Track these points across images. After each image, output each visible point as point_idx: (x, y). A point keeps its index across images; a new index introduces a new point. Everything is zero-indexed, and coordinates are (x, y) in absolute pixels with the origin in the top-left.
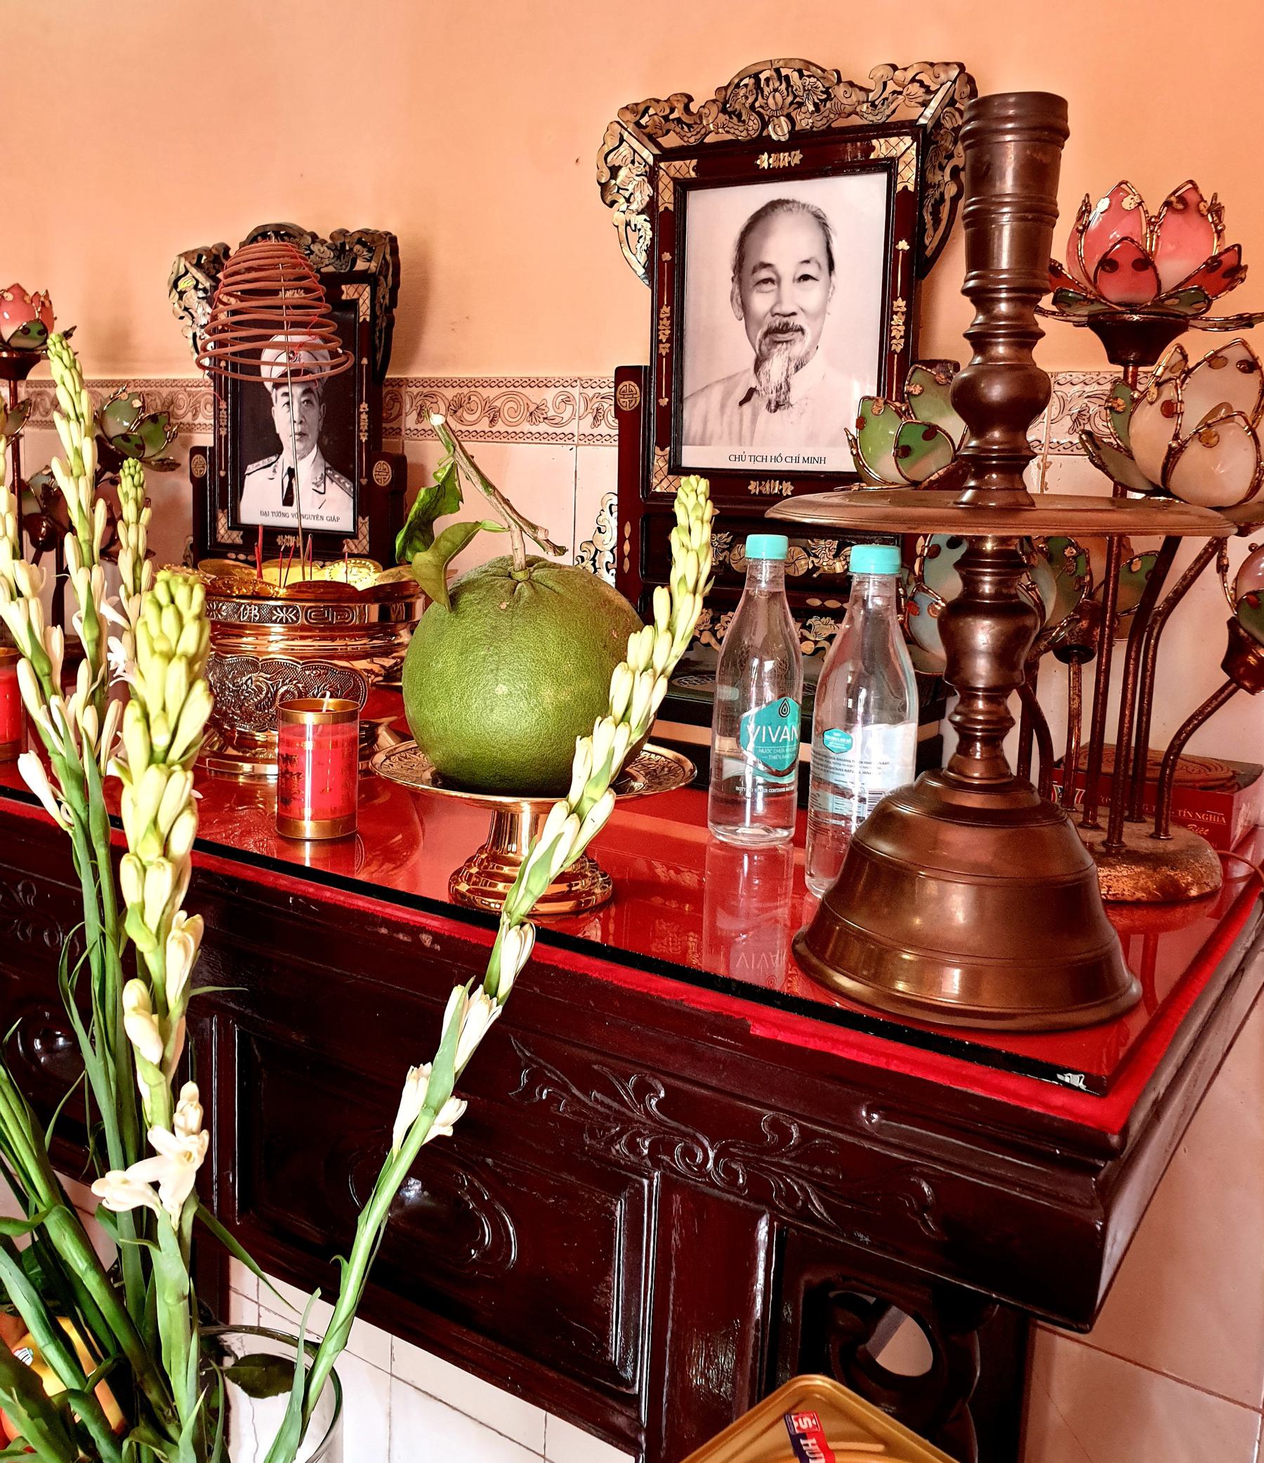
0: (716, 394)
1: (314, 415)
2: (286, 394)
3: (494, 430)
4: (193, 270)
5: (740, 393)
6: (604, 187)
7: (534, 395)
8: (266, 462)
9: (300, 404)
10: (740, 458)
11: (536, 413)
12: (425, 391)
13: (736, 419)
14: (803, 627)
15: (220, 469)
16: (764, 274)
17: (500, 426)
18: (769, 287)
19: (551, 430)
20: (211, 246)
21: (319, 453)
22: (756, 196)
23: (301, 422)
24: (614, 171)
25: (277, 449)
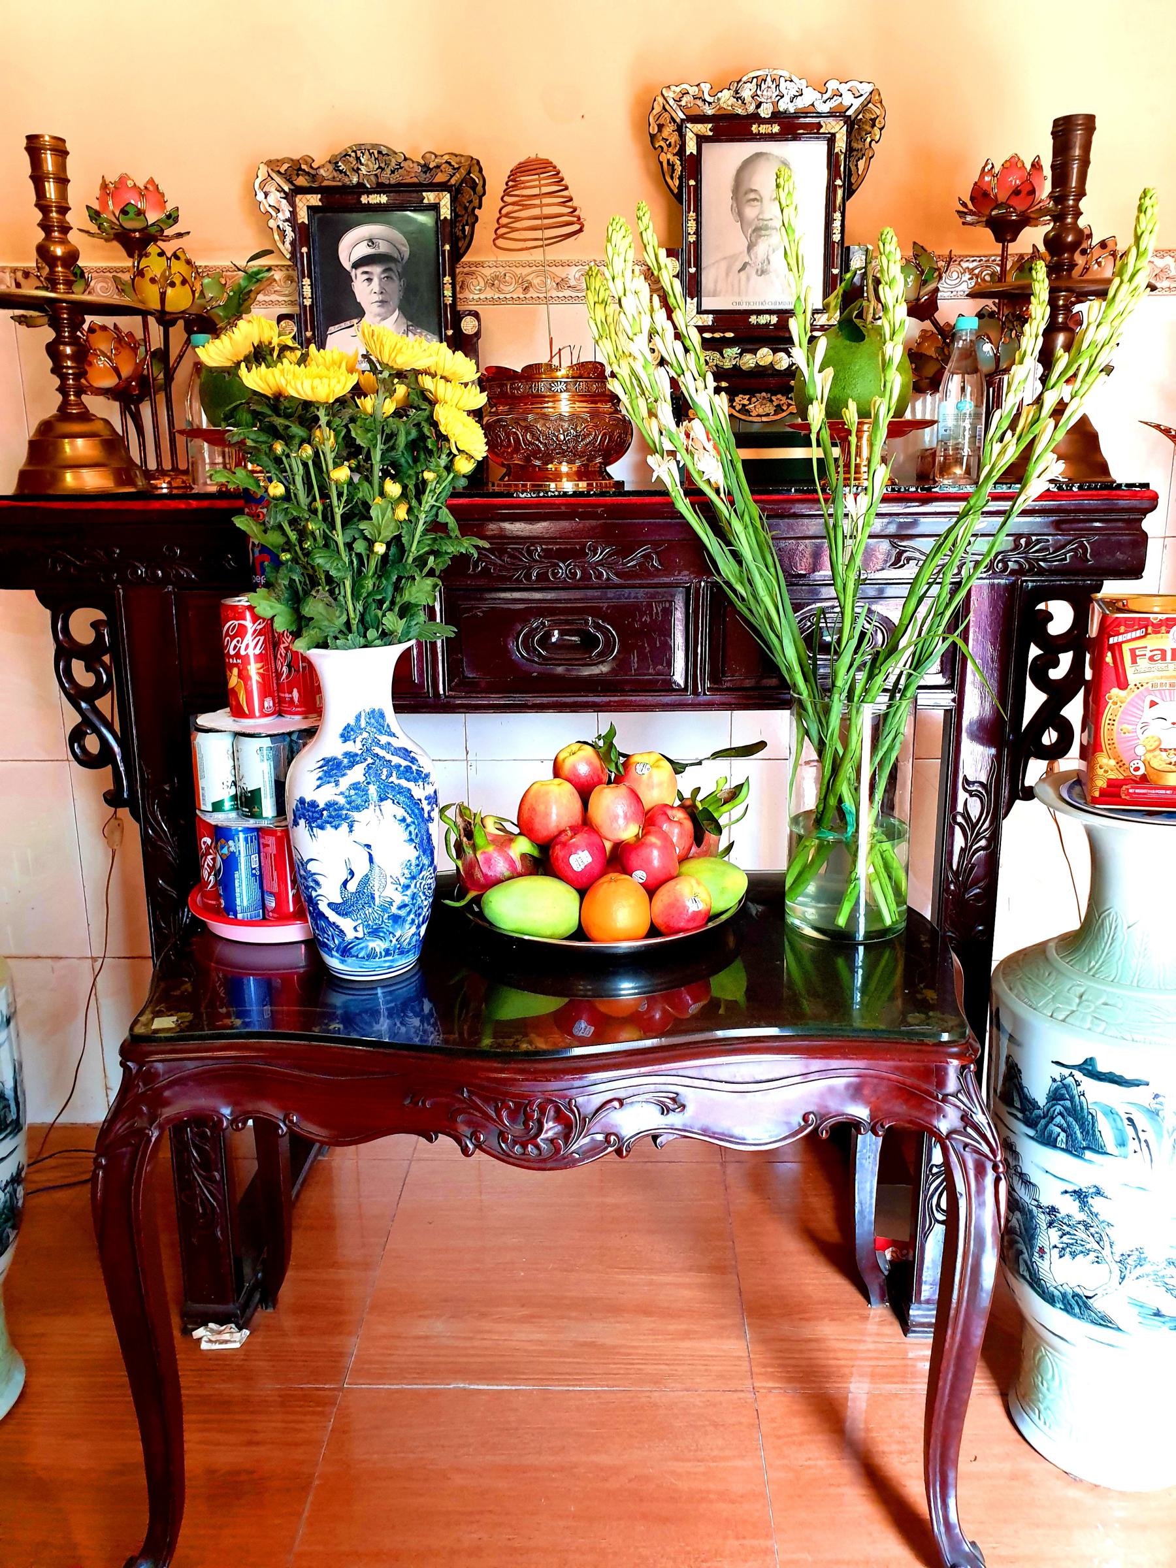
0: (723, 265)
1: (395, 287)
2: (366, 273)
3: (528, 296)
4: (274, 175)
5: (739, 265)
6: (653, 137)
7: (560, 272)
8: (348, 323)
9: (380, 280)
10: (740, 303)
11: (561, 284)
12: (466, 270)
13: (736, 283)
14: (787, 398)
15: (306, 330)
16: (752, 196)
17: (532, 293)
18: (756, 203)
19: (574, 294)
20: (298, 158)
21: (401, 315)
22: (745, 150)
23: (382, 293)
24: (661, 127)
25: (360, 313)
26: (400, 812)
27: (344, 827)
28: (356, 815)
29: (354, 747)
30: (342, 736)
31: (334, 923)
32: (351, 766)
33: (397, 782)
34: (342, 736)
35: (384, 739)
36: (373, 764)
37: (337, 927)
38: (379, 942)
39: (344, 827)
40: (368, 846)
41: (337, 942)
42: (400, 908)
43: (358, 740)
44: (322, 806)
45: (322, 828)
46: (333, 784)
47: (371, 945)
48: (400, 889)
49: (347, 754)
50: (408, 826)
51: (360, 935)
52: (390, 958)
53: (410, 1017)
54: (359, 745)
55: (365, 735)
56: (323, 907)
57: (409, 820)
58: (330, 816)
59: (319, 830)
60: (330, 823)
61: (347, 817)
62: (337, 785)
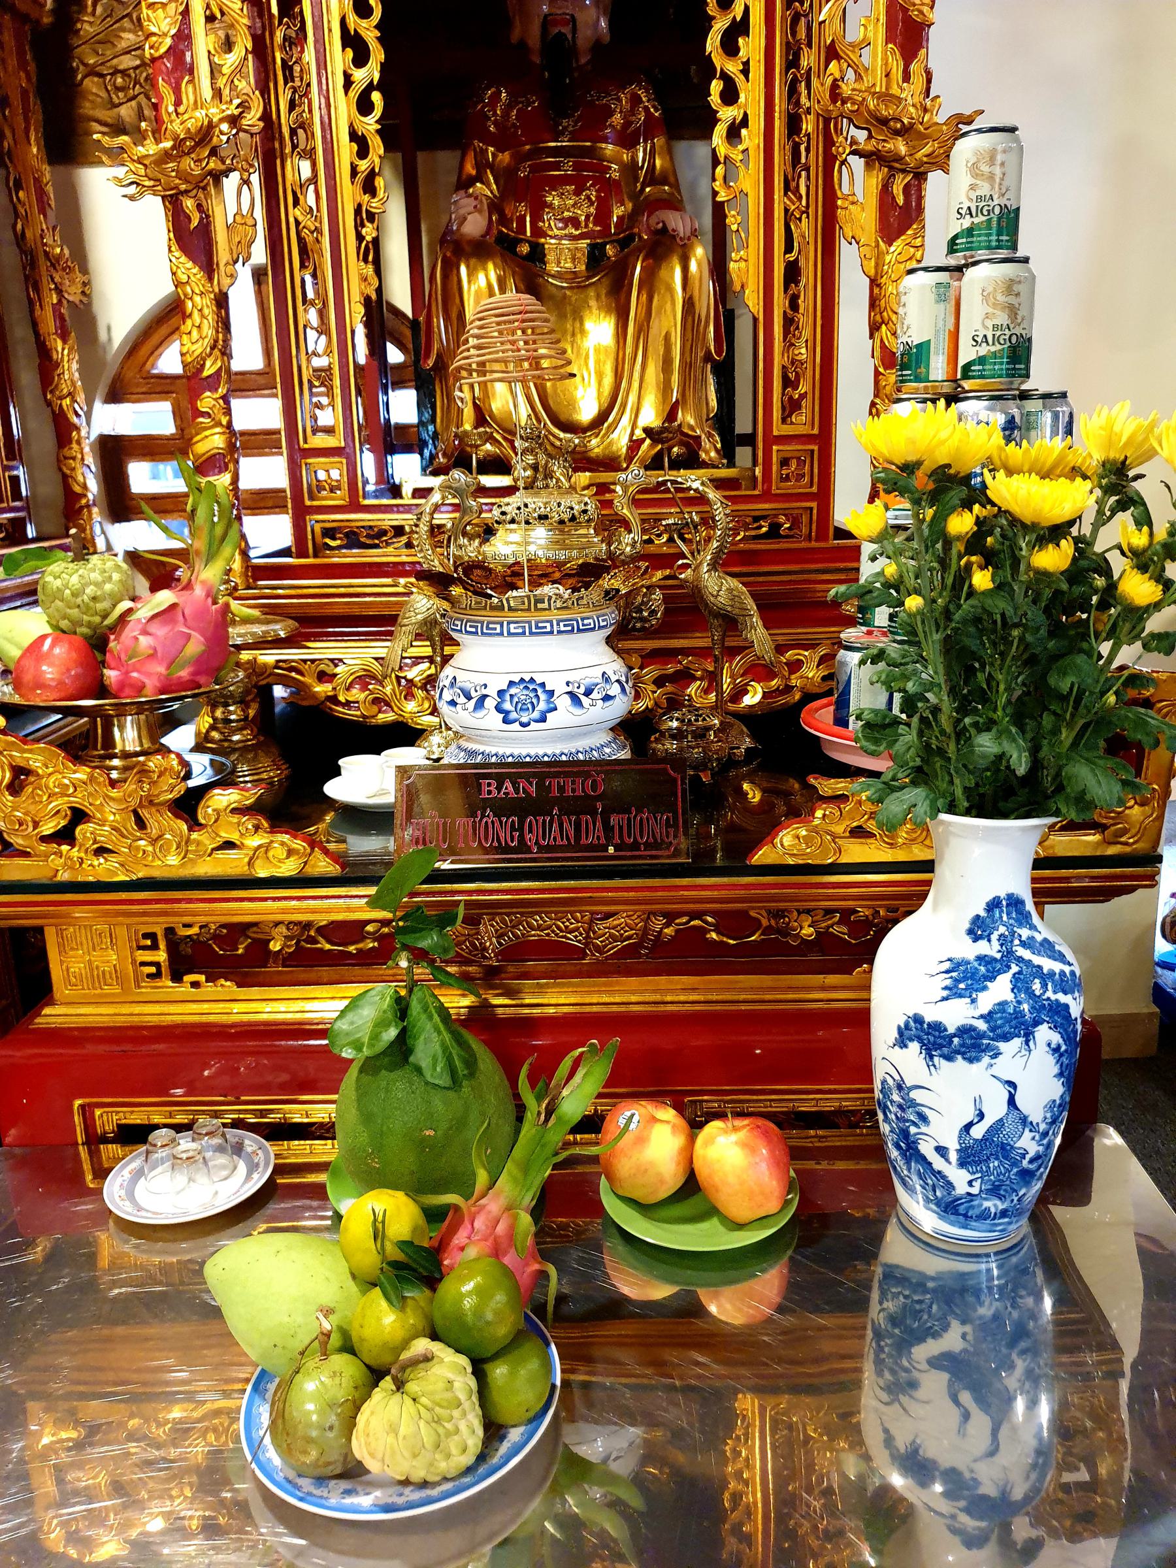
26: (1056, 1038)
28: (1002, 1046)
29: (991, 948)
30: (970, 932)
31: (939, 1172)
32: (992, 978)
33: (1053, 997)
34: (970, 932)
35: (1025, 933)
36: (1020, 973)
37: (944, 1177)
38: (998, 1203)
39: (986, 1060)
40: (1012, 1084)
41: (938, 1194)
42: (1031, 1161)
43: (994, 937)
44: (951, 1030)
45: (949, 1058)
46: (968, 1000)
47: (986, 1204)
48: (1037, 1138)
49: (980, 958)
50: (1061, 1055)
51: (975, 1190)
52: (1006, 1220)
53: (1021, 1297)
54: (996, 945)
55: (1002, 929)
56: (926, 1148)
57: (1063, 1048)
58: (963, 1045)
59: (943, 1062)
60: (963, 1054)
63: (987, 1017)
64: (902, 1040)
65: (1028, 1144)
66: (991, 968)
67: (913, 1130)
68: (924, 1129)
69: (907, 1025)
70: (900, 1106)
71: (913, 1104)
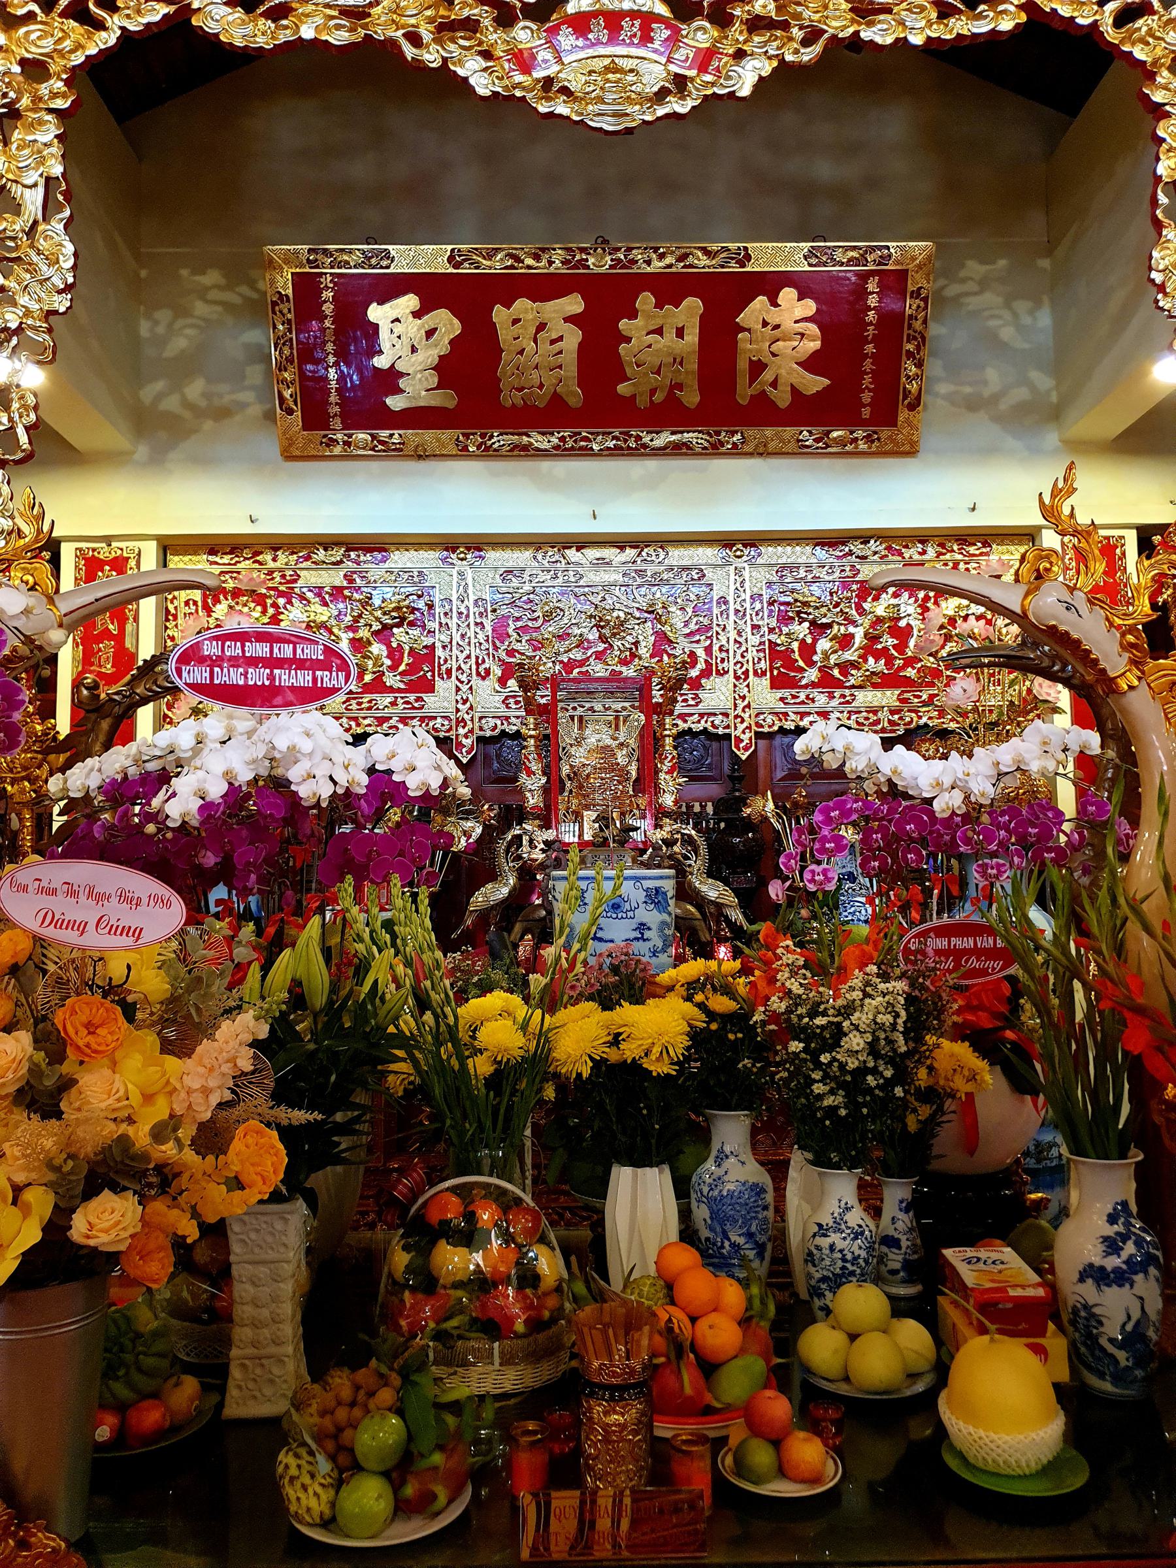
27: (1127, 1286)
29: (1119, 1228)
39: (1127, 1286)
40: (1141, 1298)
44: (1109, 1269)
45: (1109, 1285)
49: (1117, 1233)
51: (1130, 1364)
56: (1103, 1341)
61: (1129, 1279)
62: (1119, 1256)
63: (1126, 1262)
64: (1082, 1280)
65: (1151, 1333)
66: (1125, 1238)
67: (1095, 1331)
68: (1101, 1330)
69: (1085, 1270)
70: (1085, 1318)
71: (1094, 1315)
